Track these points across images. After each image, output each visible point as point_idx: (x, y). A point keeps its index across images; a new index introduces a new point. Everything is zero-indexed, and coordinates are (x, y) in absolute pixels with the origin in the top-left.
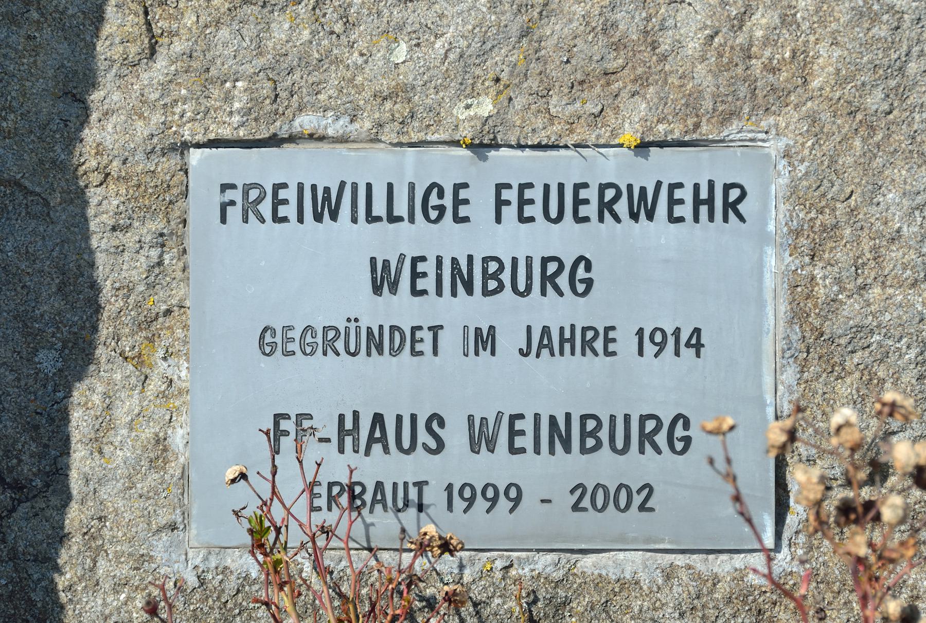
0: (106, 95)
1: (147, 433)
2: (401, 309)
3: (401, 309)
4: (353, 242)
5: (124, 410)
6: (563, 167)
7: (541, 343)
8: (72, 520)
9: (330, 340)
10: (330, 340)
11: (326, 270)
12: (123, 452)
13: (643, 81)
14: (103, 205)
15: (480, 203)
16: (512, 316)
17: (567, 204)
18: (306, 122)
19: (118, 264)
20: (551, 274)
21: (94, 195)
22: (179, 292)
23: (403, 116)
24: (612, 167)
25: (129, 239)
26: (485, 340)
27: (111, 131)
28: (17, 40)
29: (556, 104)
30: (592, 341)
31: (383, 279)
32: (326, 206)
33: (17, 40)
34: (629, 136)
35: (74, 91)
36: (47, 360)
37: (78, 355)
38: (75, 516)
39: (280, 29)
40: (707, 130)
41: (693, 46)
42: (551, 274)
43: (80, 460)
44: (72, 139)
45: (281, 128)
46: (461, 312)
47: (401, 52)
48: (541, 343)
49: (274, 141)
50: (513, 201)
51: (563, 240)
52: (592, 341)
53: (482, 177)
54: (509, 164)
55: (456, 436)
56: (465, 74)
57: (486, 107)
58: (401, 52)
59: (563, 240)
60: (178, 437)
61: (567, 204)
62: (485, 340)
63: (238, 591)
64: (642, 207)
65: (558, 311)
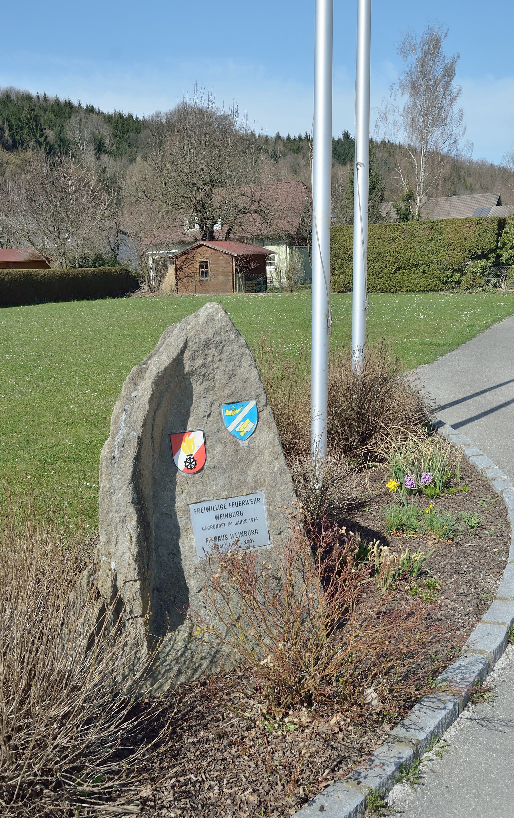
0: (177, 499)
1: (190, 544)
2: (220, 522)
3: (220, 522)
4: (212, 514)
5: (186, 542)
6: (237, 499)
7: (238, 523)
8: (189, 570)
9: (211, 527)
10: (211, 527)
11: (209, 518)
12: (187, 548)
13: (245, 486)
14: (179, 514)
15: (227, 506)
16: (234, 520)
17: (238, 504)
18: (204, 499)
19: (182, 523)
20: (238, 514)
21: (178, 514)
22: (190, 525)
23: (216, 496)
24: (243, 498)
25: (183, 519)
26: (231, 524)
27: (179, 503)
28: (165, 493)
29: (235, 491)
30: (244, 521)
31: (217, 518)
32: (208, 510)
33: (165, 493)
34: (245, 494)
35: (173, 499)
36: (175, 537)
37: (178, 536)
38: (182, 557)
39: (198, 487)
40: (254, 491)
41: (251, 481)
42: (238, 514)
43: (182, 549)
44: (174, 506)
45: (201, 500)
46: (227, 521)
47: (214, 487)
48: (238, 523)
49: (200, 502)
50: (231, 505)
51: (239, 509)
52: (244, 521)
53: (227, 502)
54: (230, 500)
55: (229, 537)
56: (223, 489)
57: (227, 493)
58: (214, 487)
59: (239, 509)
60: (194, 544)
61: (238, 504)
62: (231, 524)
63: (342, 664)
64: (248, 503)
65: (239, 518)
